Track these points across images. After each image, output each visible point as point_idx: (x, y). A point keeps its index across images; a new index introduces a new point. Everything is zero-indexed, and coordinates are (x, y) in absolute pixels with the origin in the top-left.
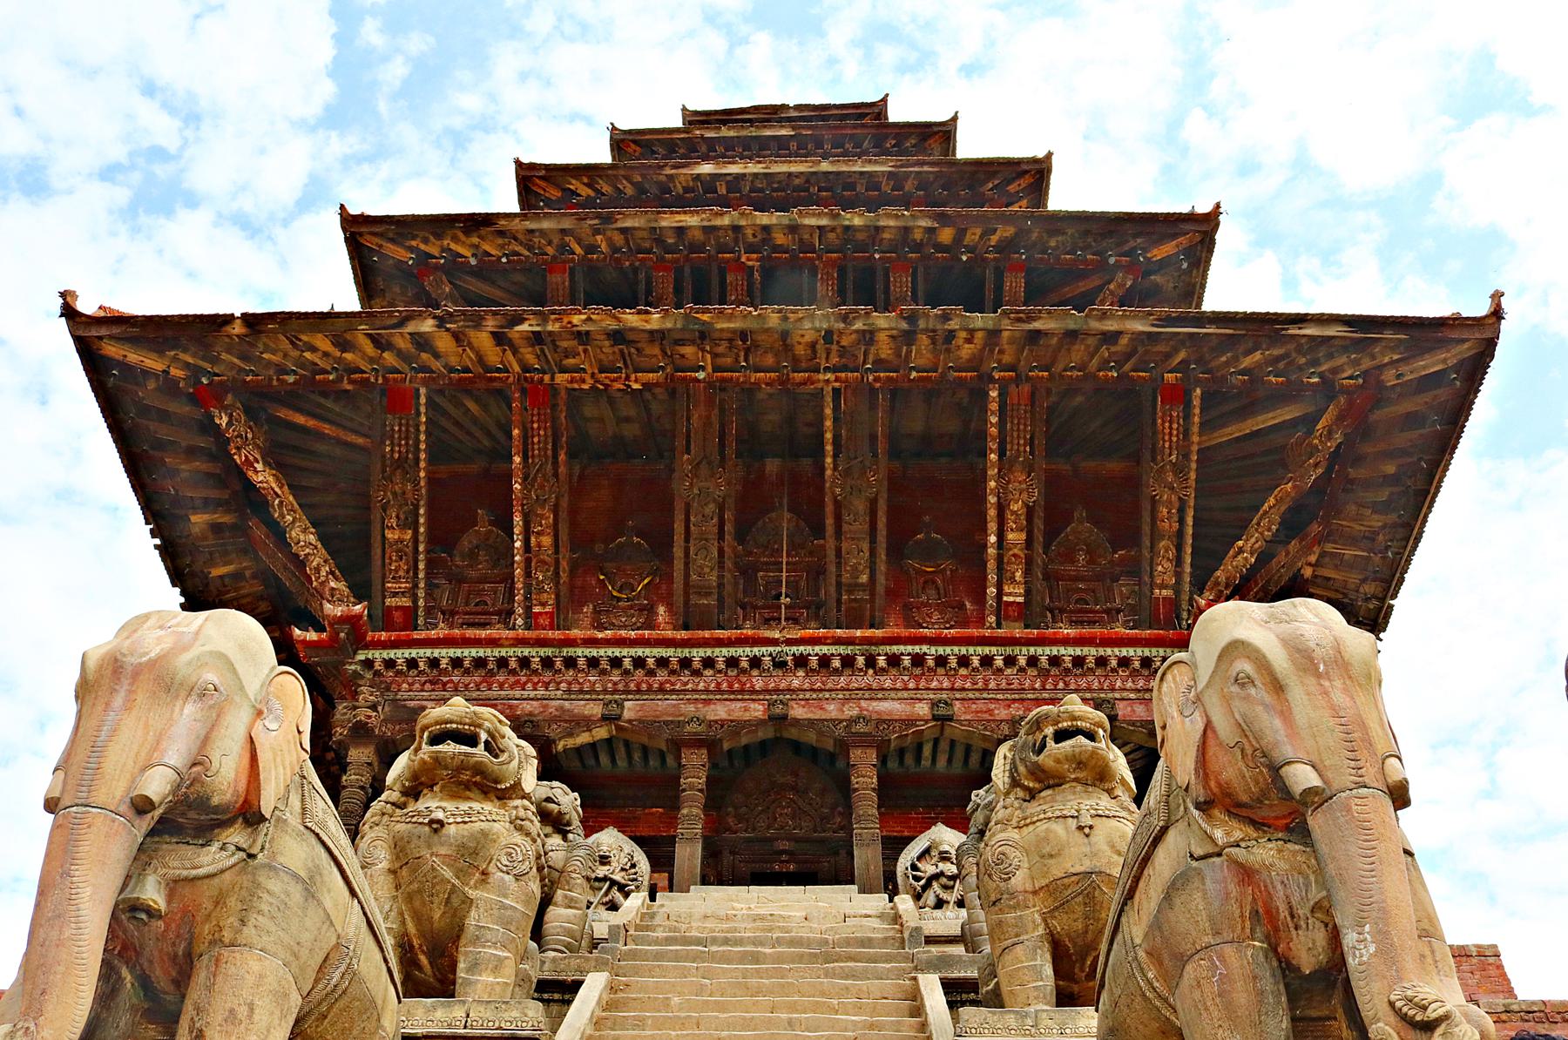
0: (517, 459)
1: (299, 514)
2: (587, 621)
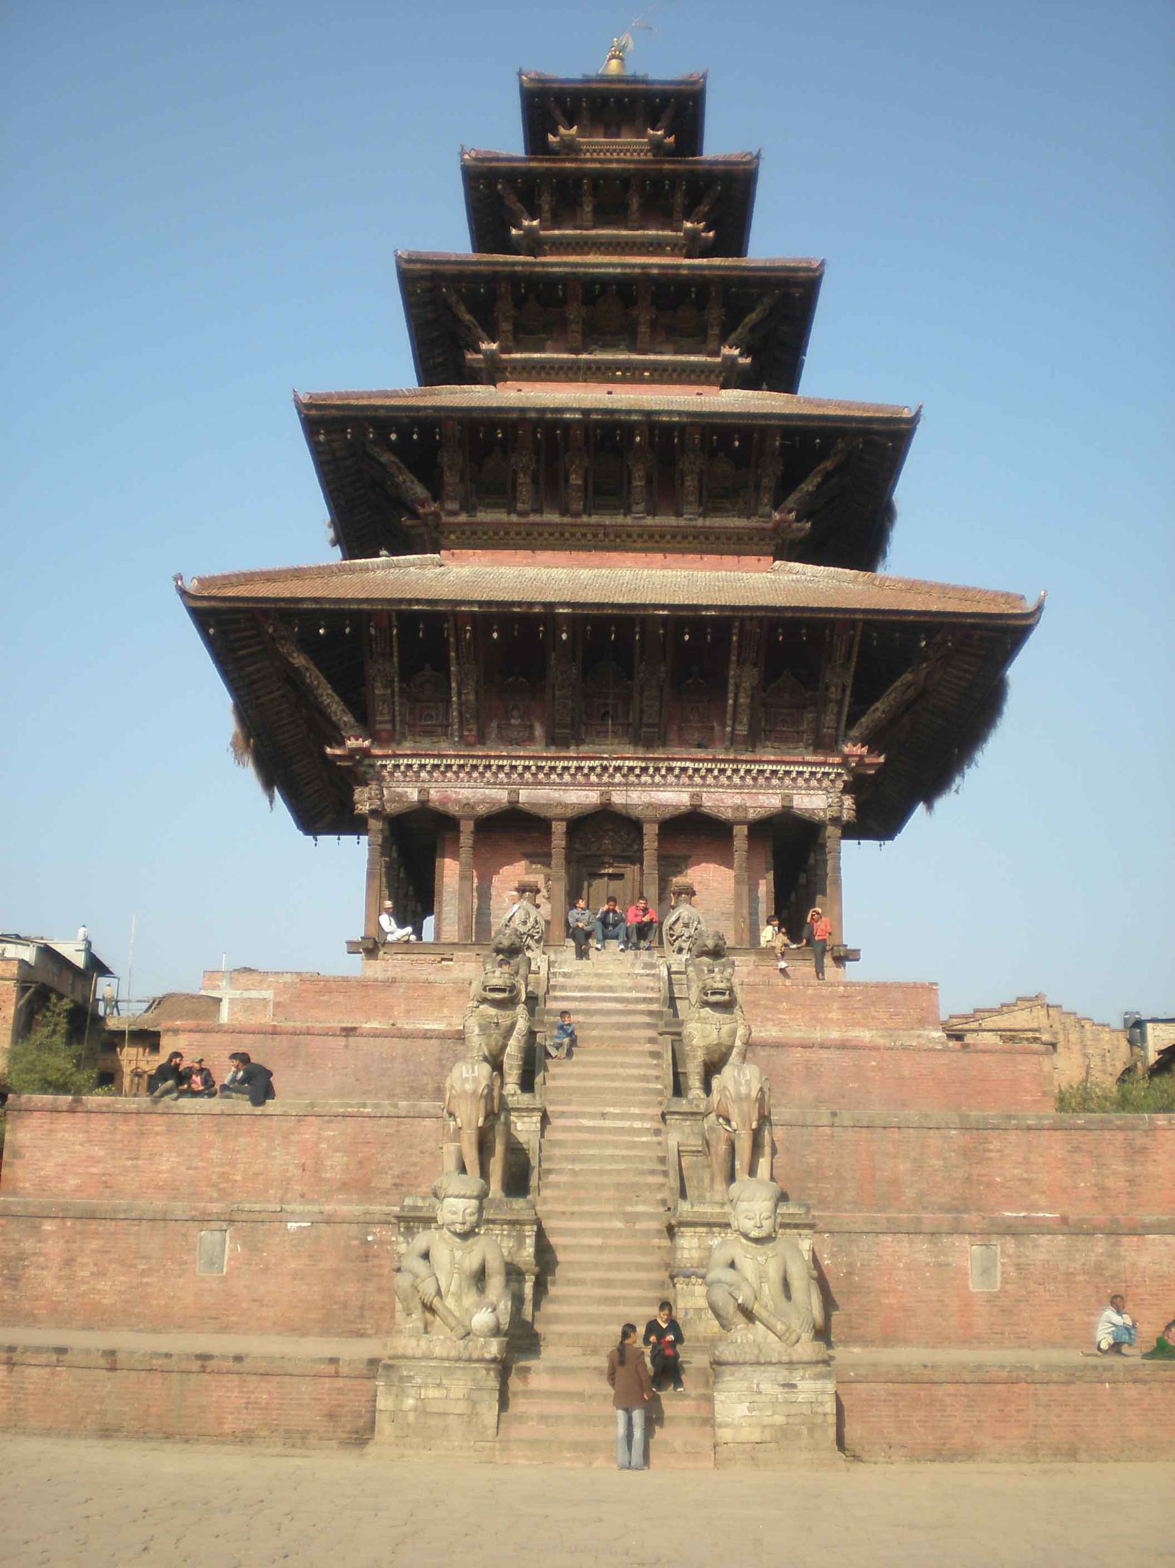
0: (453, 654)
1: (322, 678)
2: (493, 735)
